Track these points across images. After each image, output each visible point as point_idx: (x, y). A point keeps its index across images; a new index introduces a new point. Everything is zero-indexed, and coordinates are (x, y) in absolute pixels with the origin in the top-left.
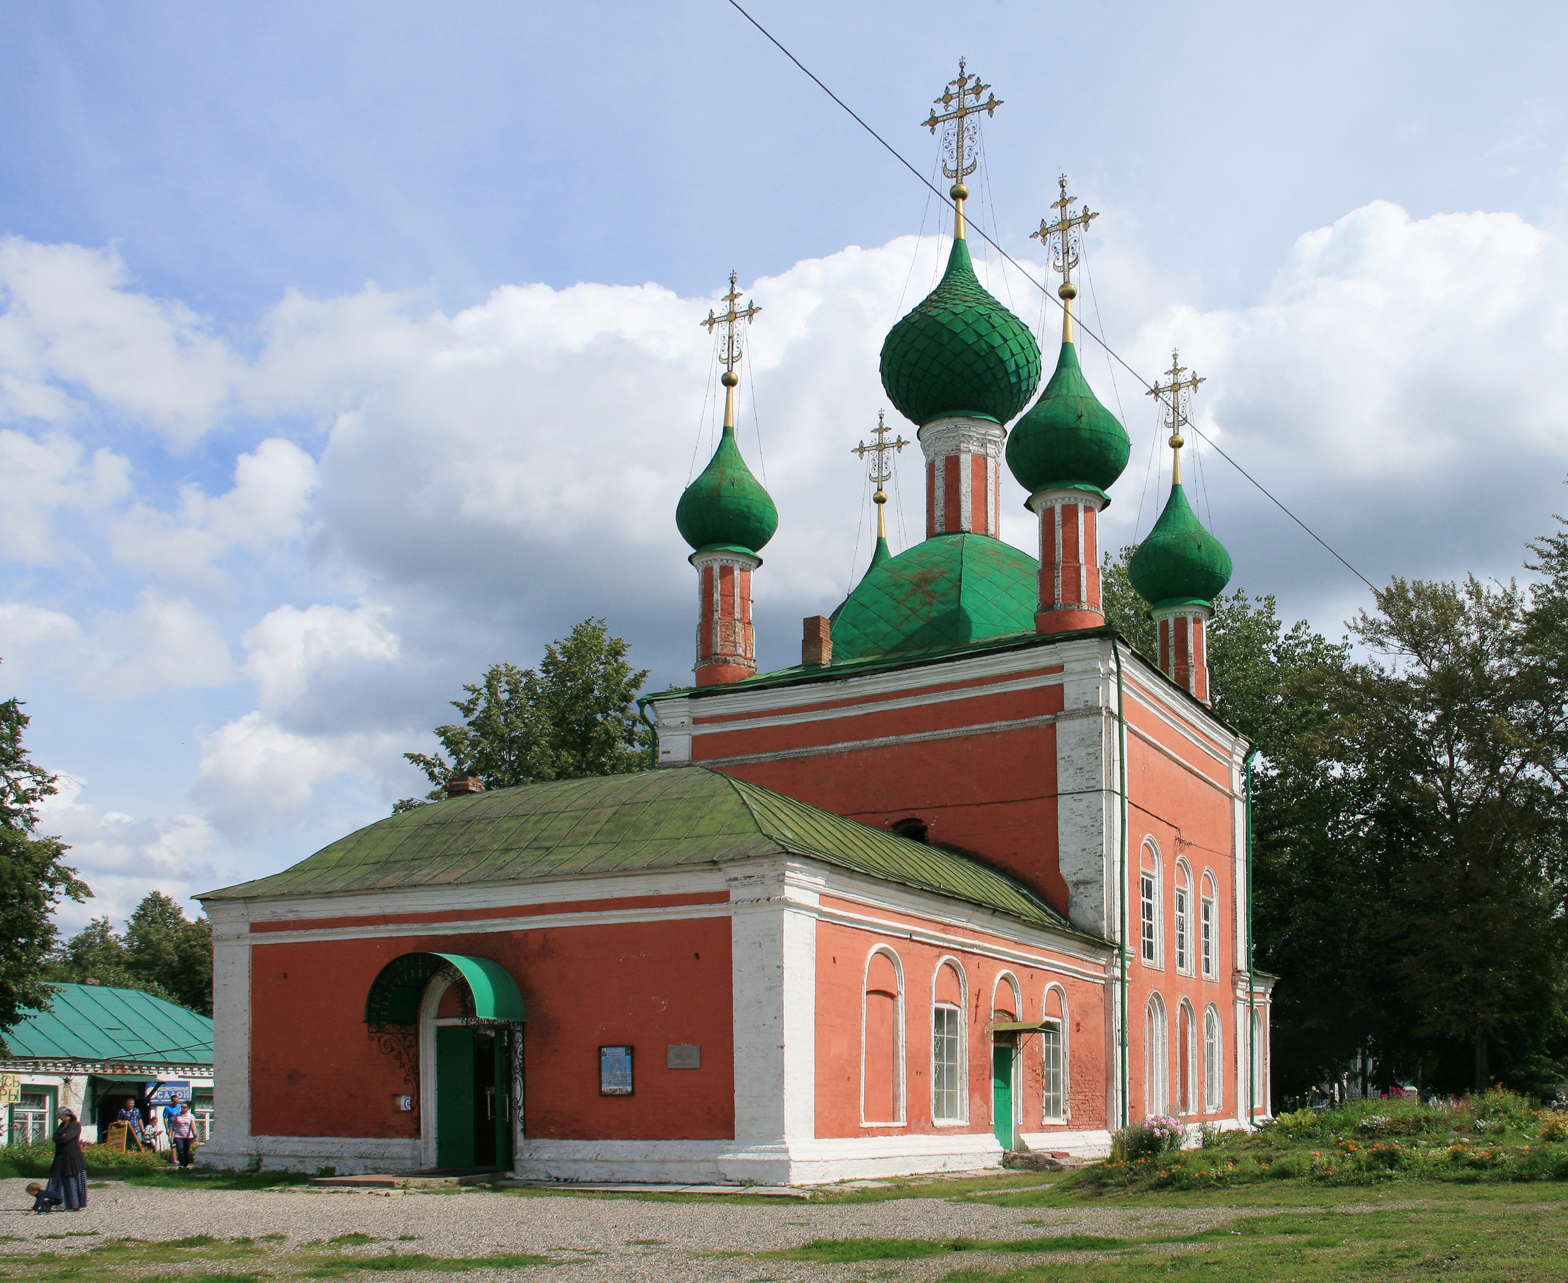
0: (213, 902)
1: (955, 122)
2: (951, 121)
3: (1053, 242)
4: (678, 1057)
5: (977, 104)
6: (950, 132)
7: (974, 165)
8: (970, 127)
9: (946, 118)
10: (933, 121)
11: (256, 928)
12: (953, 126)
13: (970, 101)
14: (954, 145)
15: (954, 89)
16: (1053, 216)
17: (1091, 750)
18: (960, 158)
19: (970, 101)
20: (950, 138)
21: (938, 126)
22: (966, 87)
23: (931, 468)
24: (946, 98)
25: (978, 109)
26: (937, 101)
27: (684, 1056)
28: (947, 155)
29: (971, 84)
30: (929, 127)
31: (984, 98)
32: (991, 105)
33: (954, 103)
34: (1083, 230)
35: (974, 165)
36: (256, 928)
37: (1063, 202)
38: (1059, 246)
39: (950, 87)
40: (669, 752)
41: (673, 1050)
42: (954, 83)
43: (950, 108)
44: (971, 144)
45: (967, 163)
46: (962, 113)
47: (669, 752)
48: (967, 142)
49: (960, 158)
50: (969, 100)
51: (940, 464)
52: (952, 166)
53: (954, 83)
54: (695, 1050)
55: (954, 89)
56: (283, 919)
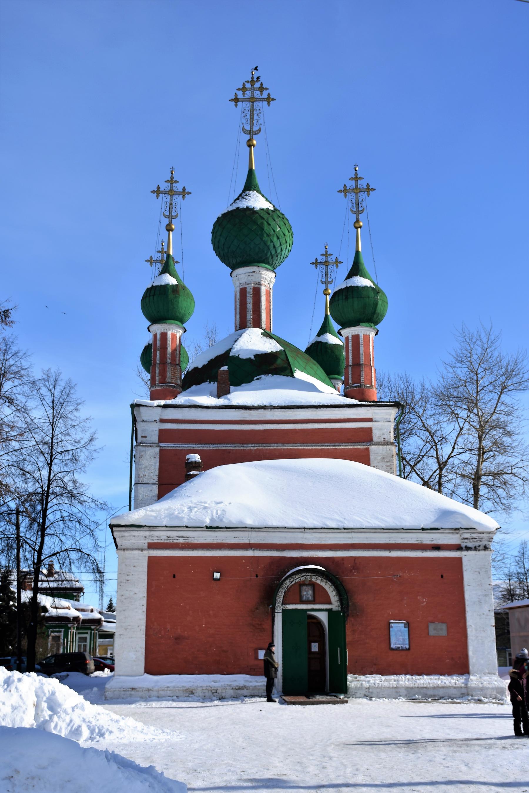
0: (123, 529)
1: (249, 104)
2: (247, 103)
3: (350, 197)
4: (435, 629)
5: (260, 97)
6: (246, 109)
7: (259, 130)
8: (258, 109)
9: (243, 100)
10: (236, 100)
11: (152, 546)
12: (248, 106)
13: (257, 94)
14: (248, 117)
15: (248, 86)
16: (351, 184)
17: (388, 464)
18: (252, 124)
19: (257, 94)
20: (246, 112)
21: (239, 104)
22: (255, 86)
23: (243, 292)
24: (244, 89)
25: (262, 100)
26: (239, 89)
27: (438, 630)
28: (244, 121)
29: (257, 85)
30: (233, 103)
31: (265, 95)
32: (269, 100)
33: (248, 94)
34: (366, 196)
35: (259, 130)
36: (152, 546)
37: (356, 178)
38: (354, 201)
39: (246, 83)
40: (146, 437)
41: (431, 627)
42: (248, 82)
43: (246, 95)
44: (257, 117)
45: (255, 128)
46: (252, 100)
47: (146, 437)
48: (256, 117)
49: (252, 124)
50: (256, 94)
51: (250, 290)
52: (248, 128)
53: (248, 82)
54: (444, 626)
55: (248, 86)
56: (175, 541)
